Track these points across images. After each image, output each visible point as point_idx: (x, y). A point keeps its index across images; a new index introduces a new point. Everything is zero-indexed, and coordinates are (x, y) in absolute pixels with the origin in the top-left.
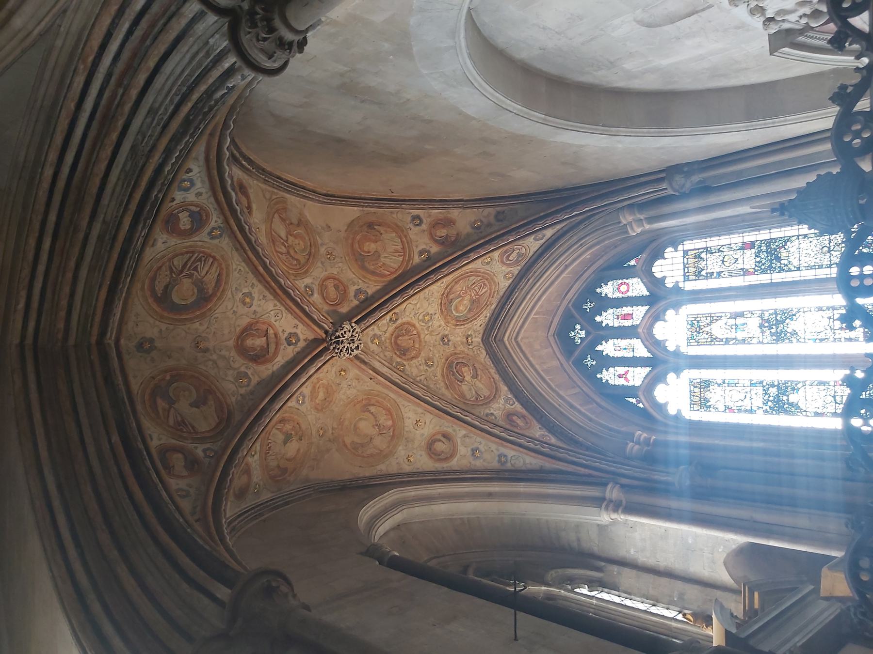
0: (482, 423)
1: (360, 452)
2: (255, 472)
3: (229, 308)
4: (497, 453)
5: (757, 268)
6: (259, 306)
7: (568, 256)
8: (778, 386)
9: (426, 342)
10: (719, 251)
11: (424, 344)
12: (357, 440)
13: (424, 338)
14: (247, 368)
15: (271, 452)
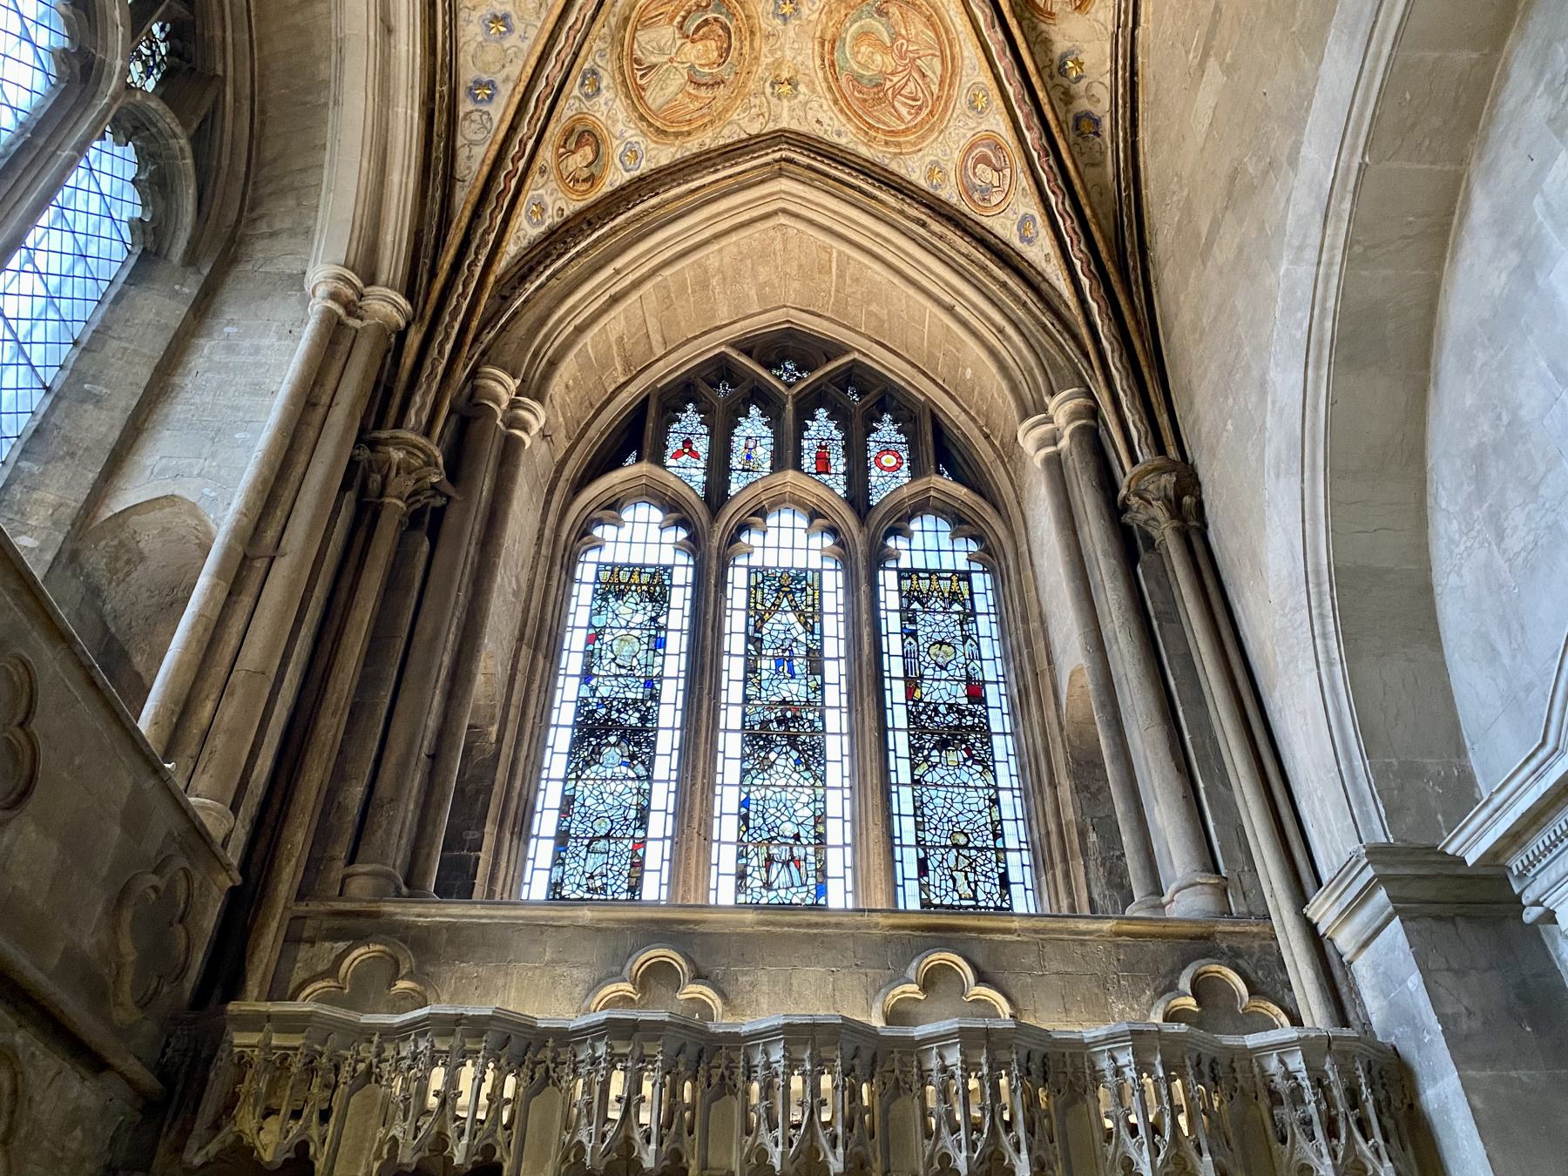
0: (572, 33)
4: (498, 79)
5: (922, 704)
7: (976, 307)
8: (645, 729)
10: (965, 638)
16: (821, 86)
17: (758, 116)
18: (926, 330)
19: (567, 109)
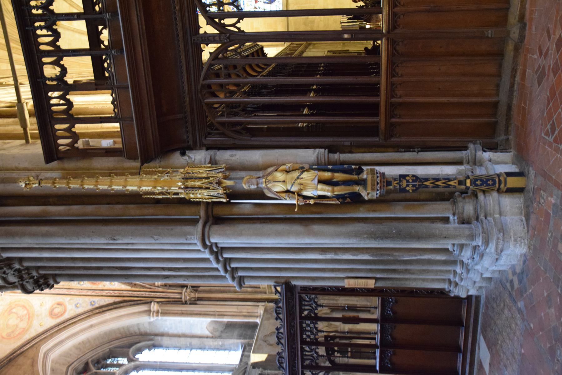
4: (89, 302)
12: (10, 331)
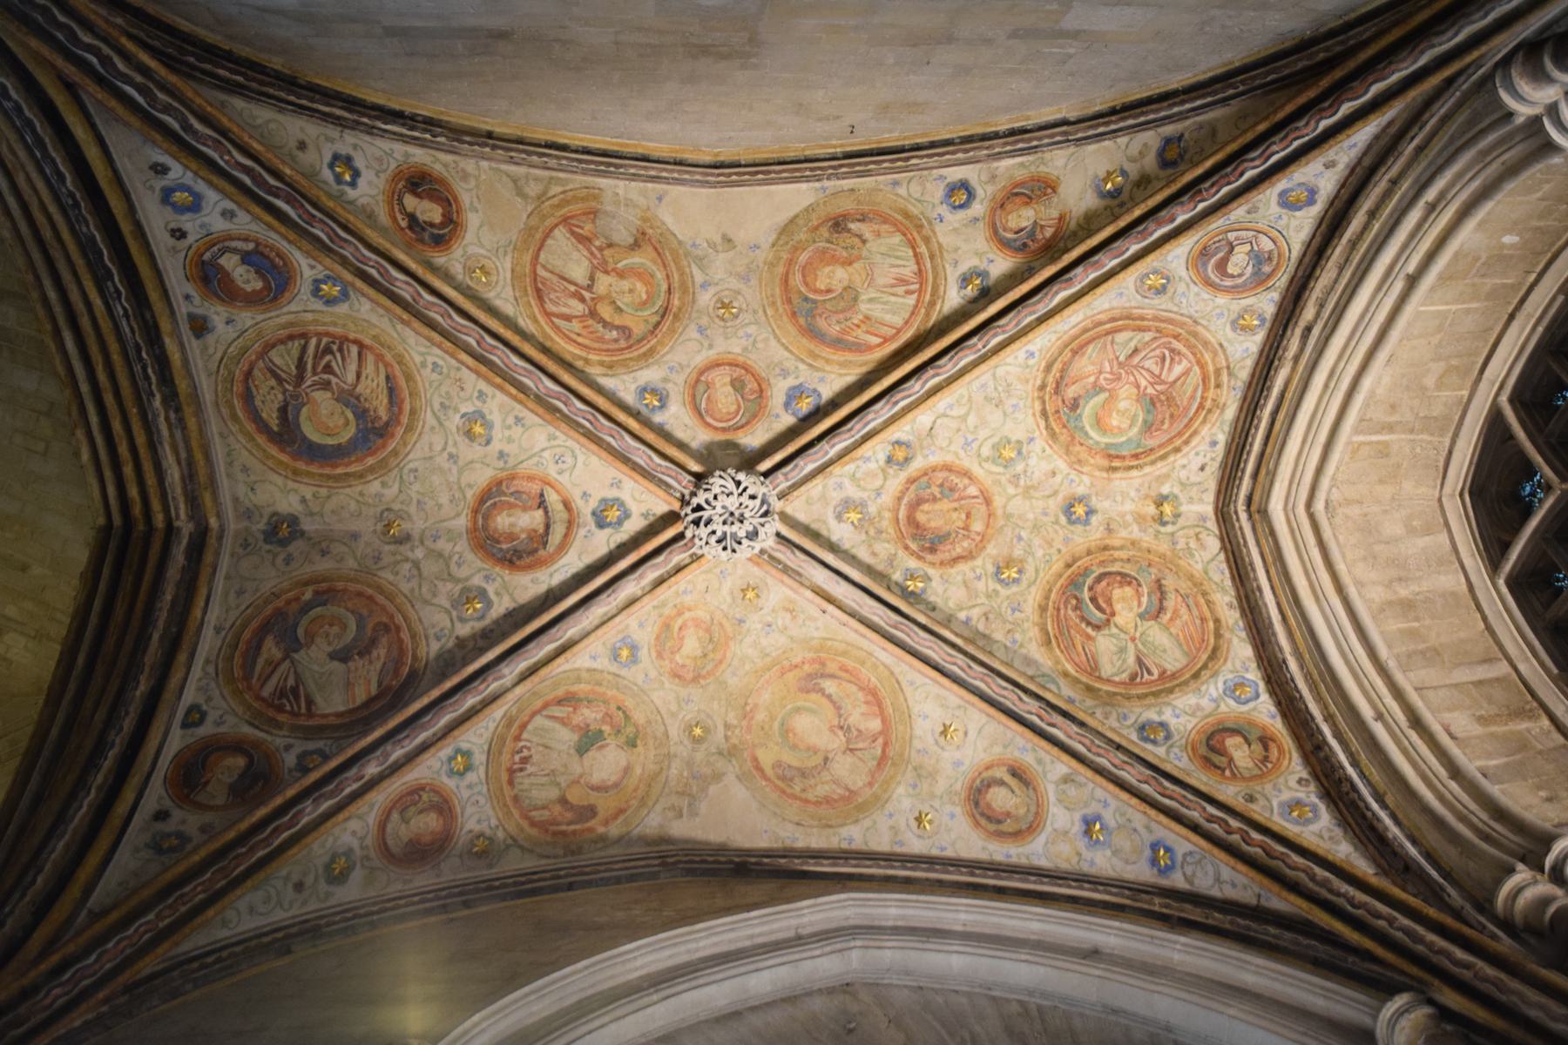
0: (1094, 749)
1: (797, 789)
2: (469, 810)
3: (439, 448)
4: (1148, 839)
6: (510, 440)
9: (1008, 516)
11: (1001, 522)
12: (790, 758)
13: (1005, 507)
14: (487, 578)
15: (530, 769)
16: (1161, 468)
17: (1198, 539)
18: (1454, 307)
19: (1178, 761)
